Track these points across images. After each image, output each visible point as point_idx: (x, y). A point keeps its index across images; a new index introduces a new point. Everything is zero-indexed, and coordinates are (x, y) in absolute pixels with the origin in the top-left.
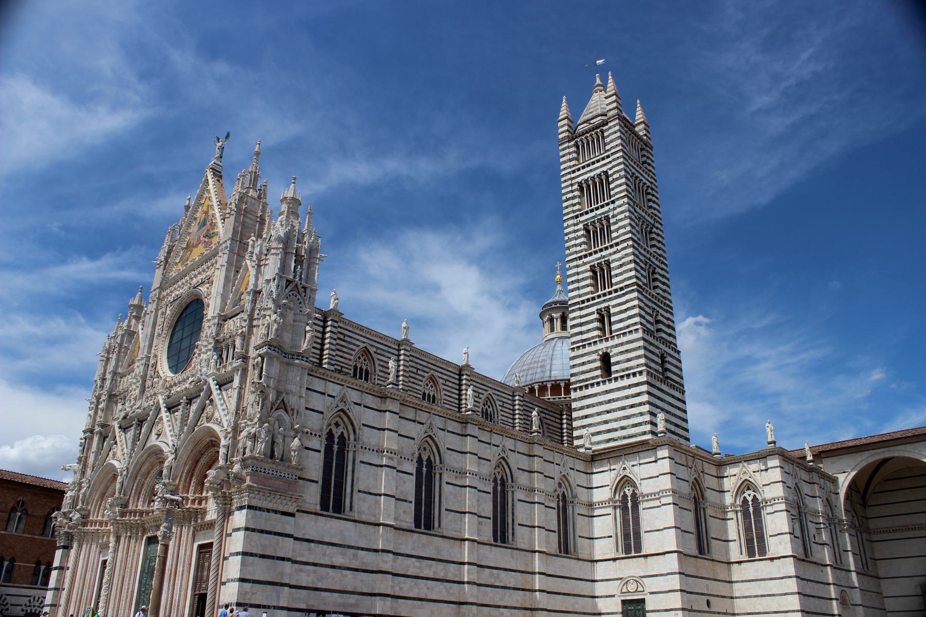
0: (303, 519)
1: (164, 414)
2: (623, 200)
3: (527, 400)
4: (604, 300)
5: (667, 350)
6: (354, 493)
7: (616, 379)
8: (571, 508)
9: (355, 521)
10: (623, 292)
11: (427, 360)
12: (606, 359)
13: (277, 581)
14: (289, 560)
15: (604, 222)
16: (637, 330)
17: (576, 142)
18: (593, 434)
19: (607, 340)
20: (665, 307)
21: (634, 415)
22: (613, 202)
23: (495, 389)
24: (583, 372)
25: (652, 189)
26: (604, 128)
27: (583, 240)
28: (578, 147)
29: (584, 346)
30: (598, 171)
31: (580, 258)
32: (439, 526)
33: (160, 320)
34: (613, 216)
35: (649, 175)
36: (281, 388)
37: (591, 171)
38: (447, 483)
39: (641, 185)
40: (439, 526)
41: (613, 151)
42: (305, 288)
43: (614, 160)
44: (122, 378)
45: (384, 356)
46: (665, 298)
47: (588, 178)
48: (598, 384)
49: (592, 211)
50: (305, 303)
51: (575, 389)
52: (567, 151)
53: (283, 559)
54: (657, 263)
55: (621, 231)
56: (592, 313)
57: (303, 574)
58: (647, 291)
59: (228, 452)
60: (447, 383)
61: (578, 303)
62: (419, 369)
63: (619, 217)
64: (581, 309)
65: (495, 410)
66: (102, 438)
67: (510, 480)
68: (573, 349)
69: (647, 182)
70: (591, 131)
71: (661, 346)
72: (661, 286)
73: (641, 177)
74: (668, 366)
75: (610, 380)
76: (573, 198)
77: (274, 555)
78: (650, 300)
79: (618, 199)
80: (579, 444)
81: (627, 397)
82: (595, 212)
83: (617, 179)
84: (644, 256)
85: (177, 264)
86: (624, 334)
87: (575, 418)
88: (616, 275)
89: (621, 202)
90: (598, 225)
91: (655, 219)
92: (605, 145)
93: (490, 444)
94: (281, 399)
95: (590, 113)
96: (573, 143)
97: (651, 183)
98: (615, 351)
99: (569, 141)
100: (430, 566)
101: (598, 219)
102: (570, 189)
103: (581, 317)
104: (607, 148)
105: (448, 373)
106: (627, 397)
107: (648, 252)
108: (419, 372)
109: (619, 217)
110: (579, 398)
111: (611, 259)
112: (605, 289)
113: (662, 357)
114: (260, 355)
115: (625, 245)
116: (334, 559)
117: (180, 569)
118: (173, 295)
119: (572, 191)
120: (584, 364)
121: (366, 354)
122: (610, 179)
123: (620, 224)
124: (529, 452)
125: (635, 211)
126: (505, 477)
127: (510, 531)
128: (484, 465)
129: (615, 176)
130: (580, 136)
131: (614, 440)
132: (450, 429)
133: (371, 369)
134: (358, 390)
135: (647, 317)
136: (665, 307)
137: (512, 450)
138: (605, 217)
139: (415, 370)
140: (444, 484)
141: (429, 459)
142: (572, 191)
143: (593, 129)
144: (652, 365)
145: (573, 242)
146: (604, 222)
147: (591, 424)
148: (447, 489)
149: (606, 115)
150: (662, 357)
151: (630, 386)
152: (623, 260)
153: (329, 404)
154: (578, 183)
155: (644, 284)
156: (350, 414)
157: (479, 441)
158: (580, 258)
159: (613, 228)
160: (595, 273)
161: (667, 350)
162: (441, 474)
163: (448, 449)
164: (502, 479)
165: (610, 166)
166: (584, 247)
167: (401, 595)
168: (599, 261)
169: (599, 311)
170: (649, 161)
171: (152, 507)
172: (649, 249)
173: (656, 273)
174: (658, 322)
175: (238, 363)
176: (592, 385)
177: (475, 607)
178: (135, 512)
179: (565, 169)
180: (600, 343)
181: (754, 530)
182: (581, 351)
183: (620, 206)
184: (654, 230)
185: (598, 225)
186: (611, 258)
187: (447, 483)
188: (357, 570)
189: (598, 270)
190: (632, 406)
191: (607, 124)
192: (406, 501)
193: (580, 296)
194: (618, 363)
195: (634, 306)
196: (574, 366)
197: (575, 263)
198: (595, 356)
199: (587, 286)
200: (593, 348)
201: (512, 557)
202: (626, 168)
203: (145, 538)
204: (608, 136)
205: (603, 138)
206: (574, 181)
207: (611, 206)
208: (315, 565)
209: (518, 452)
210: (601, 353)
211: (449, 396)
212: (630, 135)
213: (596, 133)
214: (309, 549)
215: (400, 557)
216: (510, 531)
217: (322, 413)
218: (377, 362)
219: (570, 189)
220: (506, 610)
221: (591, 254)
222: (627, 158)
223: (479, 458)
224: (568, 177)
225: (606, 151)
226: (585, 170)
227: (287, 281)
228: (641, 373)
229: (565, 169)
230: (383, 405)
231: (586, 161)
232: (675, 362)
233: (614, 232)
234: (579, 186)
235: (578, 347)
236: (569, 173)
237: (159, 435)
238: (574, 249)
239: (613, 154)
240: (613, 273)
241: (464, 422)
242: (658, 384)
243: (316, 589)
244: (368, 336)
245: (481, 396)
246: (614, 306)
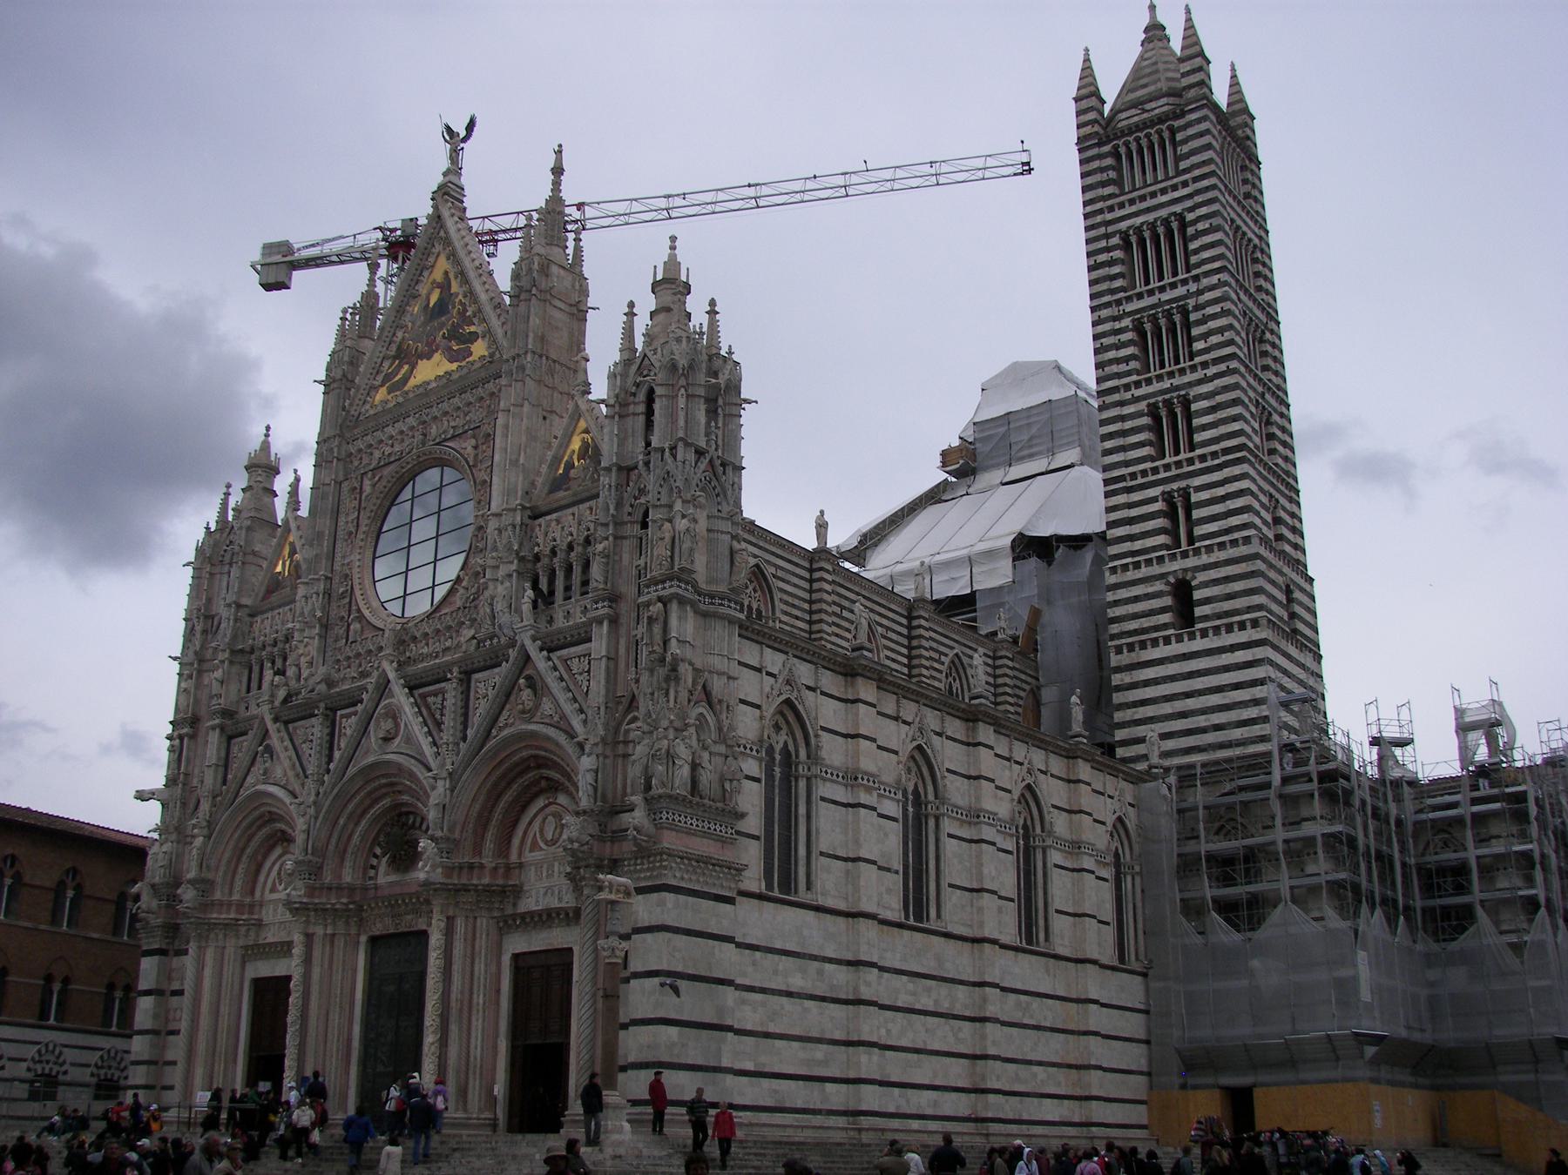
0: (746, 906)
1: (401, 697)
2: (1218, 276)
3: (1017, 666)
4: (1178, 475)
5: (1294, 576)
6: (814, 856)
7: (1204, 634)
8: (1129, 878)
9: (818, 909)
10: (1216, 462)
11: (857, 589)
12: (1182, 591)
13: (715, 1021)
14: (730, 983)
15: (1177, 318)
16: (1247, 540)
17: (1116, 147)
18: (1165, 736)
19: (1185, 555)
20: (1287, 492)
21: (1241, 702)
22: (1196, 278)
23: (965, 645)
24: (1135, 616)
25: (1262, 252)
26: (1176, 124)
27: (1130, 351)
28: (1117, 156)
29: (1137, 565)
30: (1163, 213)
31: (1127, 387)
32: (939, 916)
33: (349, 503)
34: (1197, 308)
35: (1256, 222)
36: (698, 665)
37: (1148, 210)
38: (950, 836)
39: (1245, 243)
40: (939, 916)
41: (1197, 173)
42: (723, 465)
43: (1198, 192)
44: (252, 615)
45: (788, 582)
46: (1288, 473)
47: (1142, 224)
48: (1167, 640)
49: (1151, 293)
50: (725, 496)
51: (1119, 650)
52: (1096, 164)
53: (721, 982)
54: (1273, 402)
55: (1214, 339)
56: (1154, 500)
57: (747, 1008)
58: (1261, 460)
59: (596, 781)
60: (890, 635)
61: (1122, 478)
62: (845, 608)
63: (1210, 310)
64: (1129, 490)
65: (965, 687)
66: (224, 739)
67: (1038, 830)
68: (1114, 570)
69: (1253, 237)
70: (1147, 128)
71: (1286, 570)
72: (1280, 448)
73: (1245, 228)
74: (1298, 609)
75: (1192, 637)
76: (1111, 263)
77: (708, 974)
78: (1265, 479)
79: (1207, 274)
81: (1227, 669)
82: (1158, 295)
83: (1205, 232)
84: (1255, 390)
85: (376, 388)
86: (1222, 546)
87: (1120, 704)
88: (1204, 428)
89: (1214, 279)
90: (1163, 322)
91: (1268, 313)
92: (1178, 159)
93: (1008, 759)
94: (701, 681)
95: (1145, 86)
96: (1106, 149)
97: (1260, 238)
98: (1202, 577)
99: (1099, 145)
100: (929, 990)
101: (1163, 311)
102: (1103, 244)
103: (1131, 506)
104: (1183, 165)
105: (891, 615)
106: (1227, 669)
107: (1260, 380)
108: (845, 614)
109: (1210, 310)
110: (1126, 666)
111: (1192, 394)
112: (1177, 453)
113: (1288, 592)
114: (660, 599)
115: (1223, 367)
116: (791, 980)
117: (479, 999)
118: (377, 454)
119: (1108, 249)
120: (1136, 599)
121: (757, 578)
122: (1190, 231)
123: (1212, 324)
124: (1068, 774)
125: (1239, 299)
126: (1029, 823)
127: (1041, 922)
128: (1001, 799)
129: (1201, 226)
130: (1123, 136)
132: (949, 734)
133: (767, 611)
134: (809, 662)
135: (1263, 513)
136: (1287, 492)
137: (1042, 772)
138: (1178, 307)
139: (837, 610)
140: (944, 839)
141: (916, 792)
142: (1108, 249)
143: (1152, 123)
144: (1274, 607)
145: (1112, 354)
146: (1177, 318)
147: (1152, 718)
148: (950, 846)
149: (1180, 96)
150: (1288, 592)
151: (1233, 648)
152: (1219, 399)
153: (767, 689)
154: (1120, 232)
155: (1257, 447)
156: (800, 707)
157: (997, 755)
158: (1127, 387)
159: (1195, 332)
160: (1157, 419)
161: (1294, 576)
162: (937, 818)
163: (948, 770)
164: (1025, 827)
165: (1189, 204)
166: (1134, 365)
167: (889, 1043)
168: (1167, 396)
169: (1168, 498)
170: (1255, 193)
171: (371, 878)
172: (1259, 373)
173: (1272, 424)
174: (1277, 521)
175: (603, 610)
176: (1155, 643)
177: (998, 1063)
178: (339, 888)
180: (1170, 560)
182: (1131, 575)
183: (1212, 288)
184: (1268, 335)
185: (1163, 322)
186: (1193, 392)
187: (950, 836)
188: (823, 999)
189: (1163, 413)
190: (1237, 686)
191: (1183, 114)
192: (889, 870)
193: (1127, 464)
194: (1207, 601)
195: (1242, 491)
196: (1116, 603)
197: (1116, 397)
198: (1159, 586)
199: (1141, 444)
200: (1156, 570)
201: (1047, 971)
202: (1222, 210)
203: (363, 939)
204: (1185, 141)
205: (1174, 144)
206: (1111, 229)
207: (1193, 287)
208: (763, 991)
209: (1052, 775)
210: (1172, 580)
211: (894, 660)
212: (1225, 138)
213: (1159, 132)
214: (754, 963)
215: (886, 975)
216: (1041, 922)
217: (758, 707)
218: (777, 595)
219: (1103, 244)
220: (1041, 1068)
221: (1149, 382)
222: (1223, 188)
223: (997, 787)
224: (1099, 219)
225: (1179, 173)
226: (1134, 209)
227: (696, 452)
228: (1255, 623)
230: (850, 690)
231: (1135, 190)
232: (1305, 600)
234: (1121, 238)
235: (1125, 567)
236: (1101, 211)
237: (387, 739)
238: (1115, 368)
239: (1195, 180)
240: (1196, 422)
241: (971, 717)
242: (1283, 644)
243: (767, 1035)
244: (761, 544)
246: (1199, 489)
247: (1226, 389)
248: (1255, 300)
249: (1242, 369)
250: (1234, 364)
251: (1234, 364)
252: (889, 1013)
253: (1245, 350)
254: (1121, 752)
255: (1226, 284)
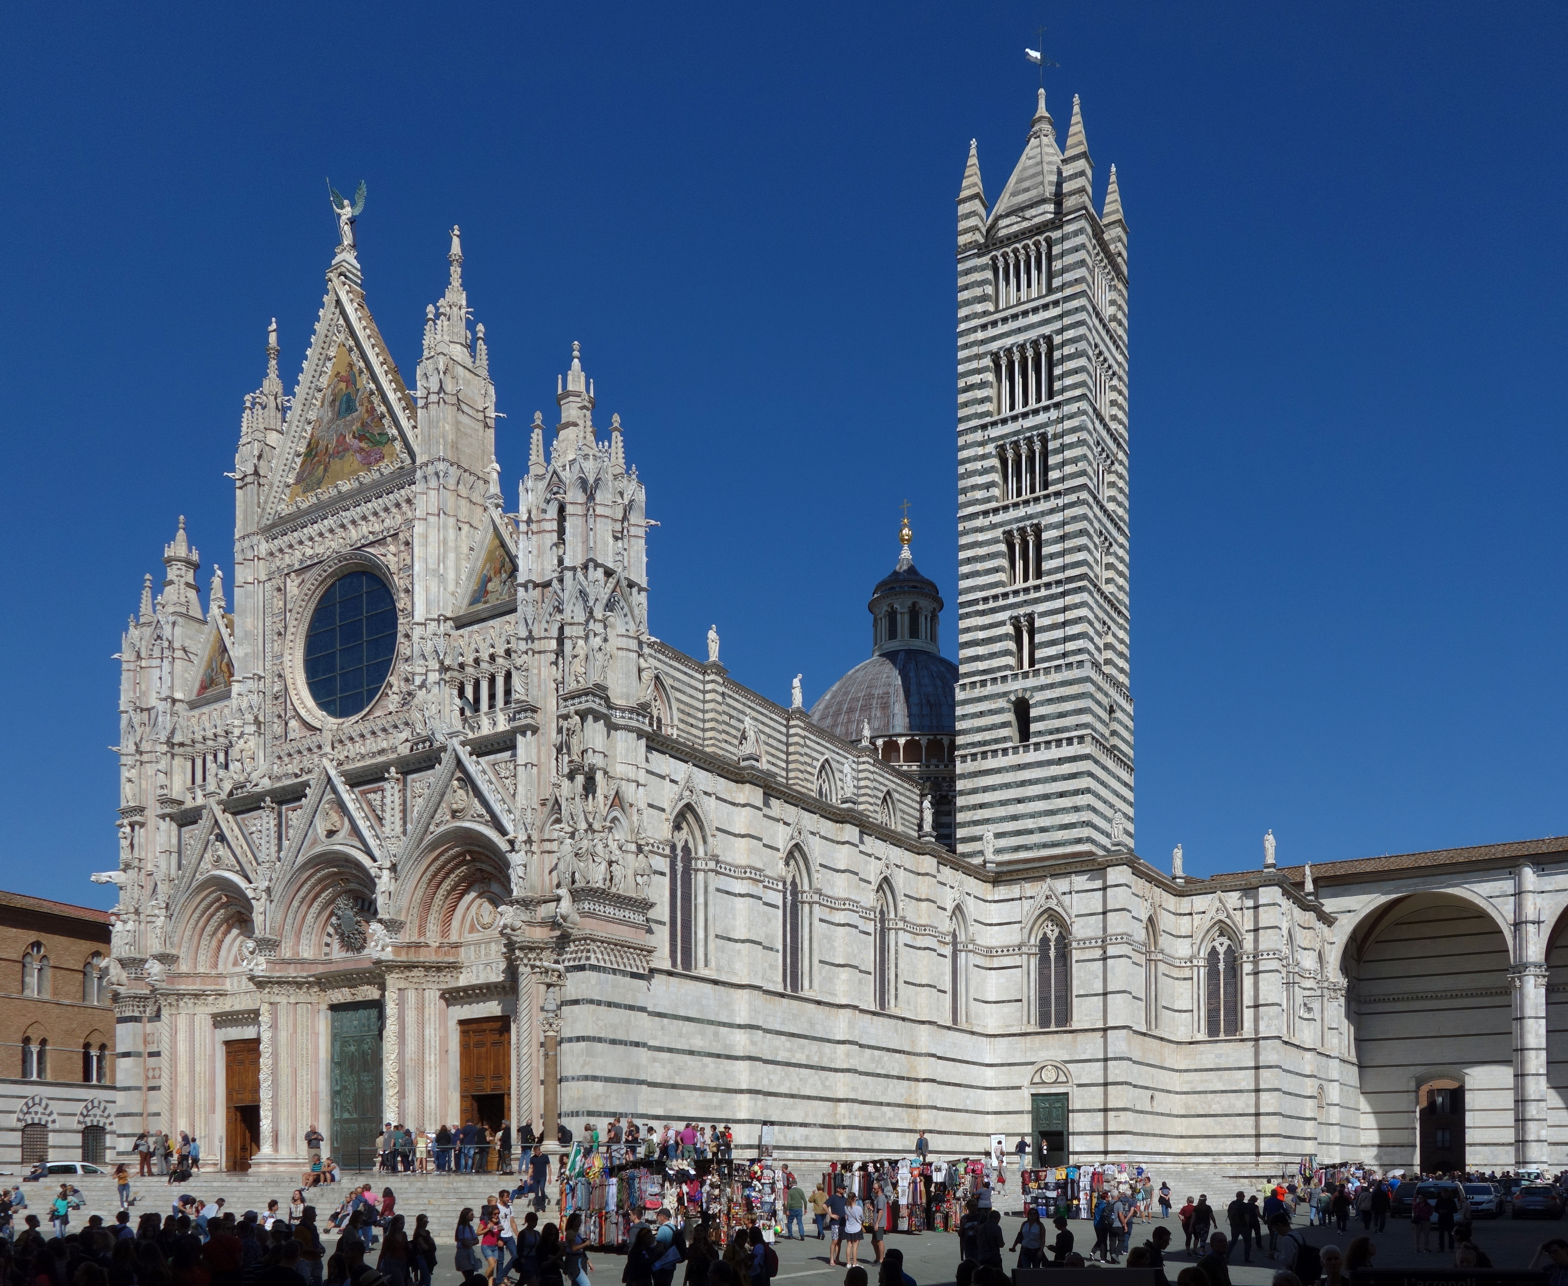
18: (998, 836)
49: (1015, 418)
55: (1069, 469)
80: (966, 850)
115: (1073, 498)
125: (1095, 429)
131: (1026, 848)
138: (1038, 435)
152: (1068, 529)
159: (1052, 460)
179: (967, 318)
181: (1222, 996)
188: (719, 1056)
206: (982, 349)
224: (972, 338)
229: (967, 318)
233: (1053, 469)
236: (974, 330)
245: (815, 763)
247: (1075, 519)
248: (1109, 430)
249: (1091, 500)
250: (1084, 495)
251: (1084, 495)
252: (770, 1067)
253: (1095, 480)
254: (961, 848)
255: (1085, 413)
